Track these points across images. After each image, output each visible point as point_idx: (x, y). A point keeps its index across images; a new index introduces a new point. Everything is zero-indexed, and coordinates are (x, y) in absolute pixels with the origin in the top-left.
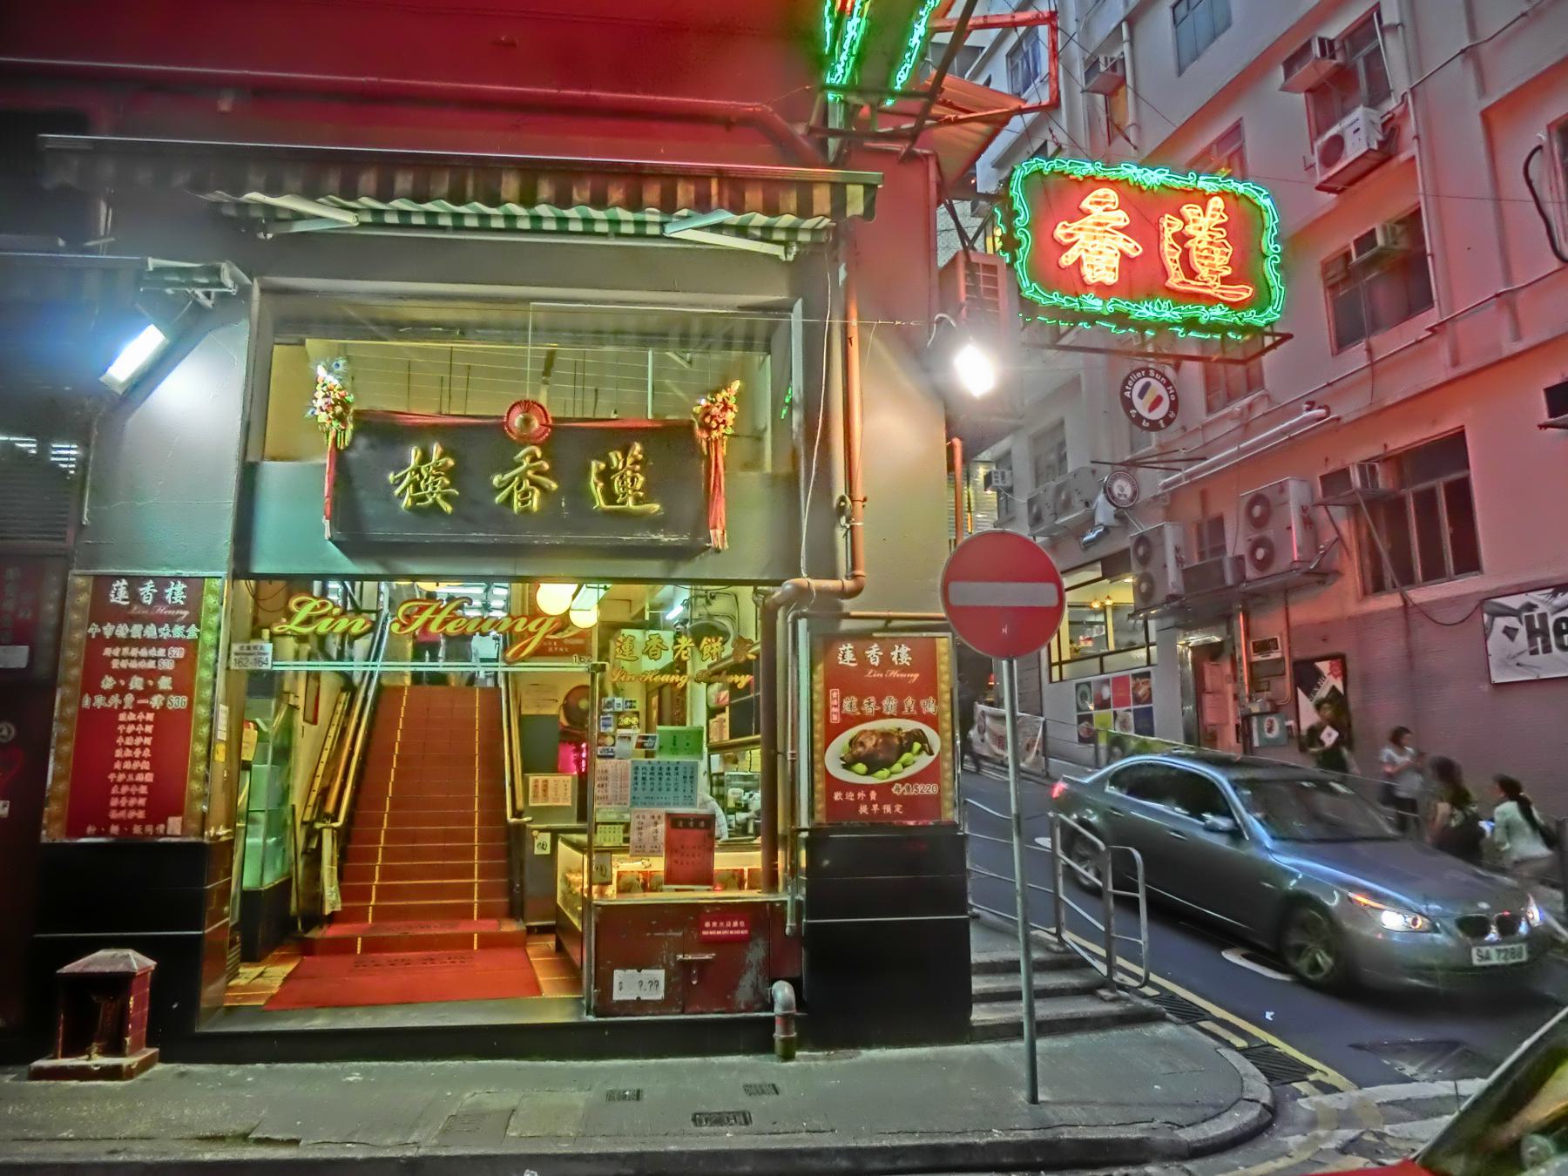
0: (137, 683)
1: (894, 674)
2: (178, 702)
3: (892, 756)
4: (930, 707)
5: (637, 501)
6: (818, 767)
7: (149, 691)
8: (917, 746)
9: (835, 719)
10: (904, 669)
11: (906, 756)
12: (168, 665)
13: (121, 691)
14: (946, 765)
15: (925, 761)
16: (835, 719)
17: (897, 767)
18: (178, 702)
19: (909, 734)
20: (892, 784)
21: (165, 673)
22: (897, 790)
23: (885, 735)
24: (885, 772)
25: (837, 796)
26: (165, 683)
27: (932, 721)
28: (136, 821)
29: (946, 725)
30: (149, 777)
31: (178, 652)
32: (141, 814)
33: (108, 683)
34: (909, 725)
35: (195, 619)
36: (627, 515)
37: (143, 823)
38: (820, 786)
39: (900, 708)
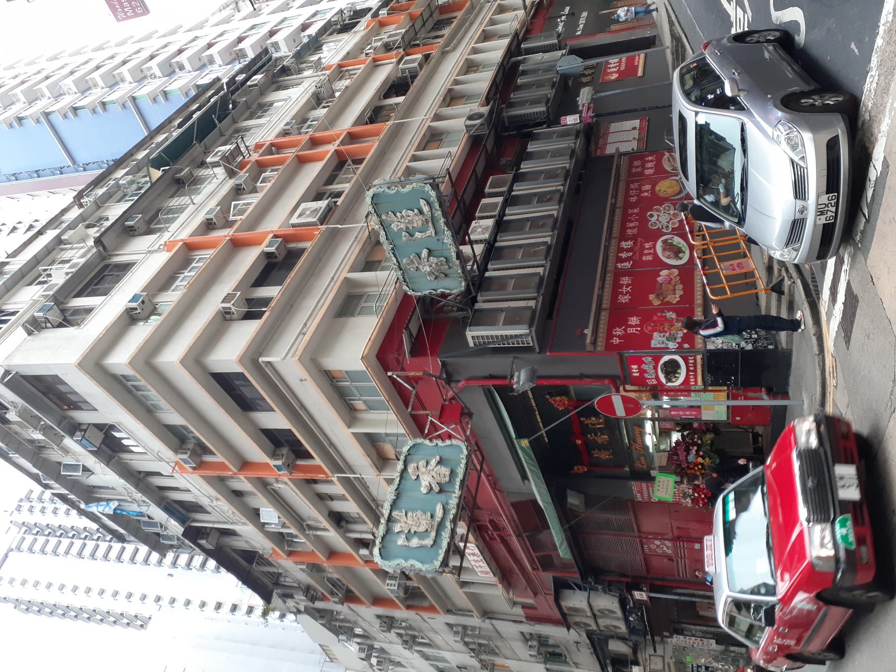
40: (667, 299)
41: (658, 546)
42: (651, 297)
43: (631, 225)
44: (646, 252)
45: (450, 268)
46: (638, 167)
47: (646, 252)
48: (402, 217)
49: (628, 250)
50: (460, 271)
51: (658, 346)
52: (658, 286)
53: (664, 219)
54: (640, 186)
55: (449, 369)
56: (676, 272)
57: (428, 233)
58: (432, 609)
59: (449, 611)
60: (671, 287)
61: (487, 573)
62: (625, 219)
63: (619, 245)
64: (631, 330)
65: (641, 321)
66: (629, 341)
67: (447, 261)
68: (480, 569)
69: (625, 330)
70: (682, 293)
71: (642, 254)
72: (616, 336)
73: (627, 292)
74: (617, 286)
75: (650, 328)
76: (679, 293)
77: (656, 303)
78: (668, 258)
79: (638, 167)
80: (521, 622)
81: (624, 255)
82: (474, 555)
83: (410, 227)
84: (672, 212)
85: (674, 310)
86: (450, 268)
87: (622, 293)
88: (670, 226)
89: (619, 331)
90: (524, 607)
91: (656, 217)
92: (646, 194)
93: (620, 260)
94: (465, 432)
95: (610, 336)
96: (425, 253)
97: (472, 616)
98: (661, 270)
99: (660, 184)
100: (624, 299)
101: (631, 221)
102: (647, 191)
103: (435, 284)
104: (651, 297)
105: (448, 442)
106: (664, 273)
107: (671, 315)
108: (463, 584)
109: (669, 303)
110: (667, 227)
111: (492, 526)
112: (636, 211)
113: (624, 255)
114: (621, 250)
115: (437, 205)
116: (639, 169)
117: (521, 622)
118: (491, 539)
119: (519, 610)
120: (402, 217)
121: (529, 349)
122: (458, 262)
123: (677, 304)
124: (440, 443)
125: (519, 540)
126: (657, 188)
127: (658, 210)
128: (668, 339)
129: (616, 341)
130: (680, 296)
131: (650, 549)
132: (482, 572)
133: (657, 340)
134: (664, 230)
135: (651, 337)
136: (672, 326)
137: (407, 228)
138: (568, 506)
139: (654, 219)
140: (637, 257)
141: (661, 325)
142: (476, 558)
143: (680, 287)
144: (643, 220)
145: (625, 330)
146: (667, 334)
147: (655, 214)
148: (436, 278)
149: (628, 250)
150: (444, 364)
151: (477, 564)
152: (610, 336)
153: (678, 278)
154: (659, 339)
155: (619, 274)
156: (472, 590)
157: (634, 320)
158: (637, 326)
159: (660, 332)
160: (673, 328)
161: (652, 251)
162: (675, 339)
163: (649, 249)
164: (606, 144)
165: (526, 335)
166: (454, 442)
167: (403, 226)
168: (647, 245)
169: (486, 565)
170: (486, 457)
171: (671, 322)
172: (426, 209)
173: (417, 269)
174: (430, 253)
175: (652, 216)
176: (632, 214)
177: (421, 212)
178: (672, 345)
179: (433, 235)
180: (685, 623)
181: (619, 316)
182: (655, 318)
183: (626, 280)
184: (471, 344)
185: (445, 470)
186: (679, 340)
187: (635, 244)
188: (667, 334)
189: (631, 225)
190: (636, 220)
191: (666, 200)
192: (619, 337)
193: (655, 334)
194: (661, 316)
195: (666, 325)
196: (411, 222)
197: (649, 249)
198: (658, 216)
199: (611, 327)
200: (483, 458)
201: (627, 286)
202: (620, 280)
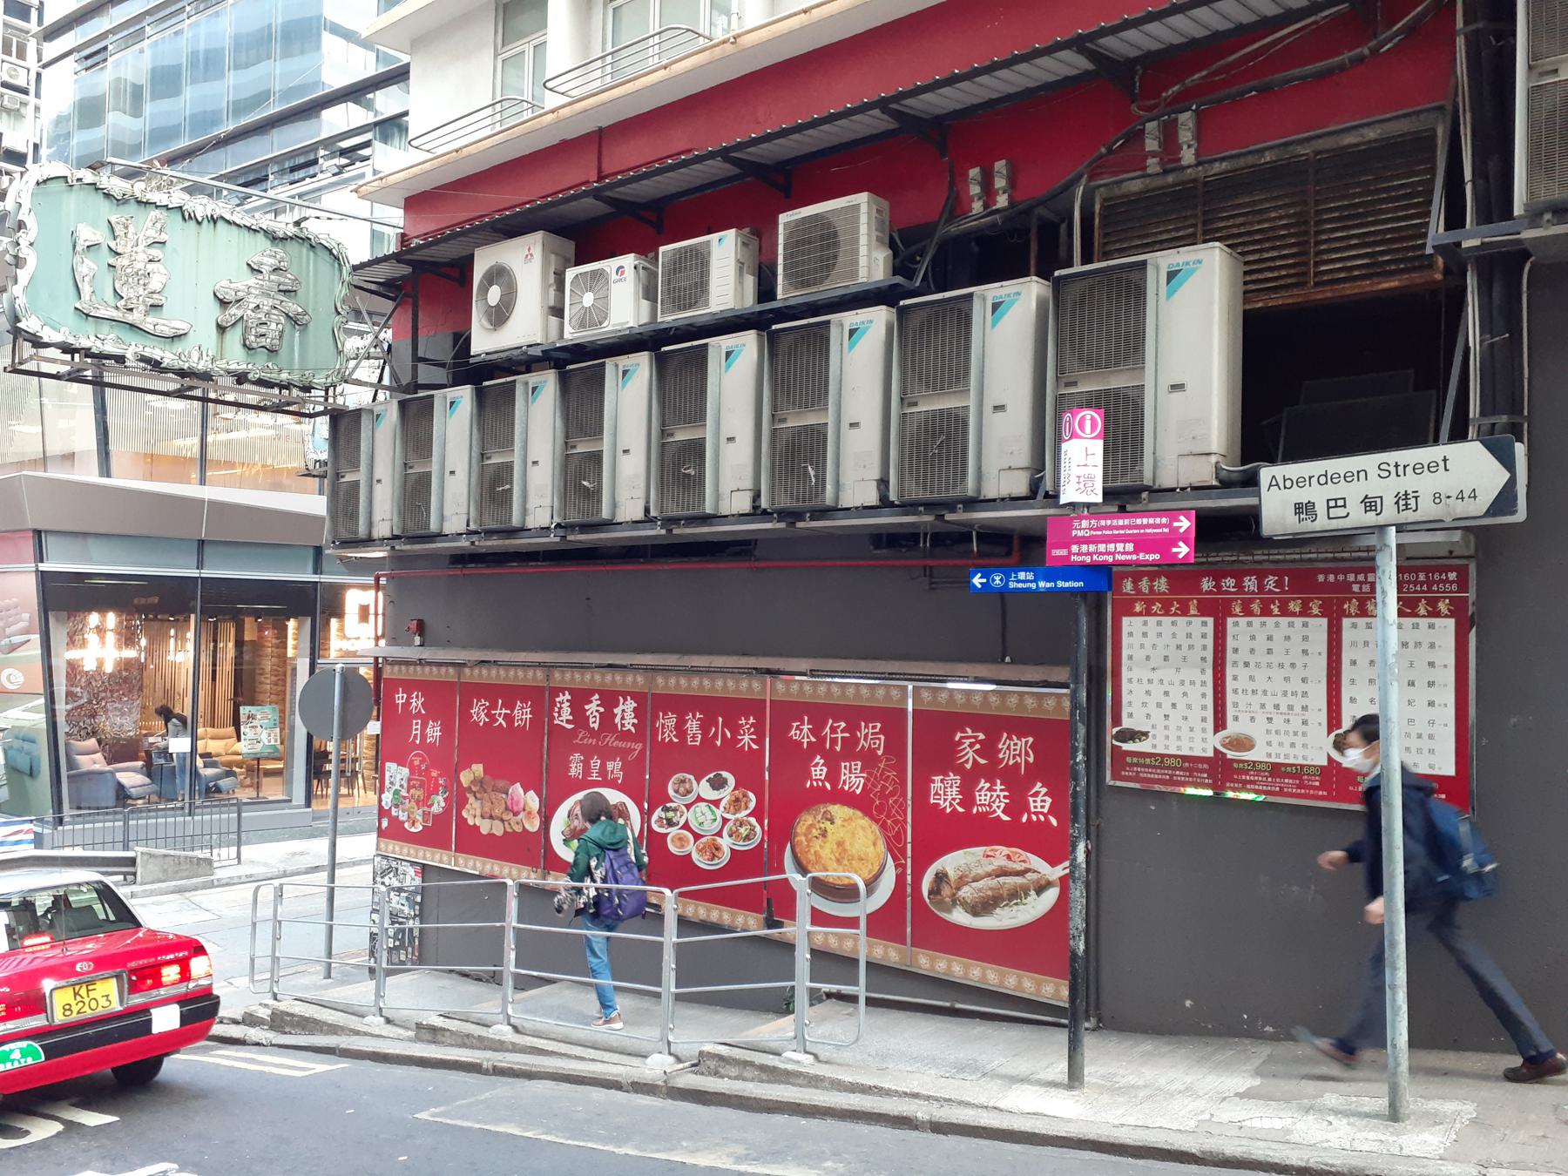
40: (471, 799)
42: (478, 769)
43: (693, 726)
44: (596, 763)
46: (989, 749)
47: (596, 763)
49: (607, 718)
51: (387, 775)
52: (501, 784)
53: (702, 818)
54: (869, 760)
56: (534, 826)
60: (497, 812)
62: (711, 708)
63: (625, 695)
64: (416, 726)
65: (432, 745)
66: (395, 721)
69: (418, 715)
70: (484, 831)
71: (588, 753)
72: (409, 698)
73: (493, 718)
74: (509, 694)
75: (416, 763)
76: (485, 827)
77: (465, 778)
79: (989, 749)
81: (593, 708)
84: (725, 842)
85: (447, 811)
87: (494, 706)
88: (673, 831)
89: (417, 703)
92: (819, 770)
93: (580, 698)
95: (409, 686)
98: (539, 794)
99: (866, 822)
100: (479, 713)
101: (704, 727)
102: (833, 776)
104: (478, 769)
106: (533, 801)
107: (438, 804)
109: (462, 802)
110: (670, 823)
112: (746, 739)
113: (593, 708)
114: (610, 699)
116: (969, 756)
123: (462, 821)
126: (839, 811)
127: (736, 803)
128: (396, 792)
129: (400, 698)
130: (476, 828)
133: (396, 774)
134: (658, 813)
135: (401, 763)
136: (417, 802)
139: (704, 789)
140: (583, 739)
141: (423, 785)
143: (498, 830)
144: (703, 761)
145: (418, 715)
146: (404, 793)
147: (726, 794)
149: (607, 718)
152: (409, 686)
153: (518, 829)
154: (399, 777)
155: (541, 698)
157: (434, 732)
158: (424, 736)
159: (409, 780)
160: (413, 804)
161: (594, 777)
162: (397, 806)
163: (603, 771)
164: (1218, 611)
168: (614, 766)
171: (425, 802)
175: (718, 784)
176: (736, 730)
178: (387, 797)
181: (445, 698)
182: (434, 774)
183: (523, 714)
186: (394, 812)
187: (626, 735)
188: (404, 793)
189: (693, 726)
190: (707, 741)
191: (781, 832)
192: (407, 704)
193: (406, 771)
194: (437, 786)
195: (418, 793)
197: (603, 771)
198: (716, 803)
199: (425, 687)
201: (509, 718)
202: (524, 701)
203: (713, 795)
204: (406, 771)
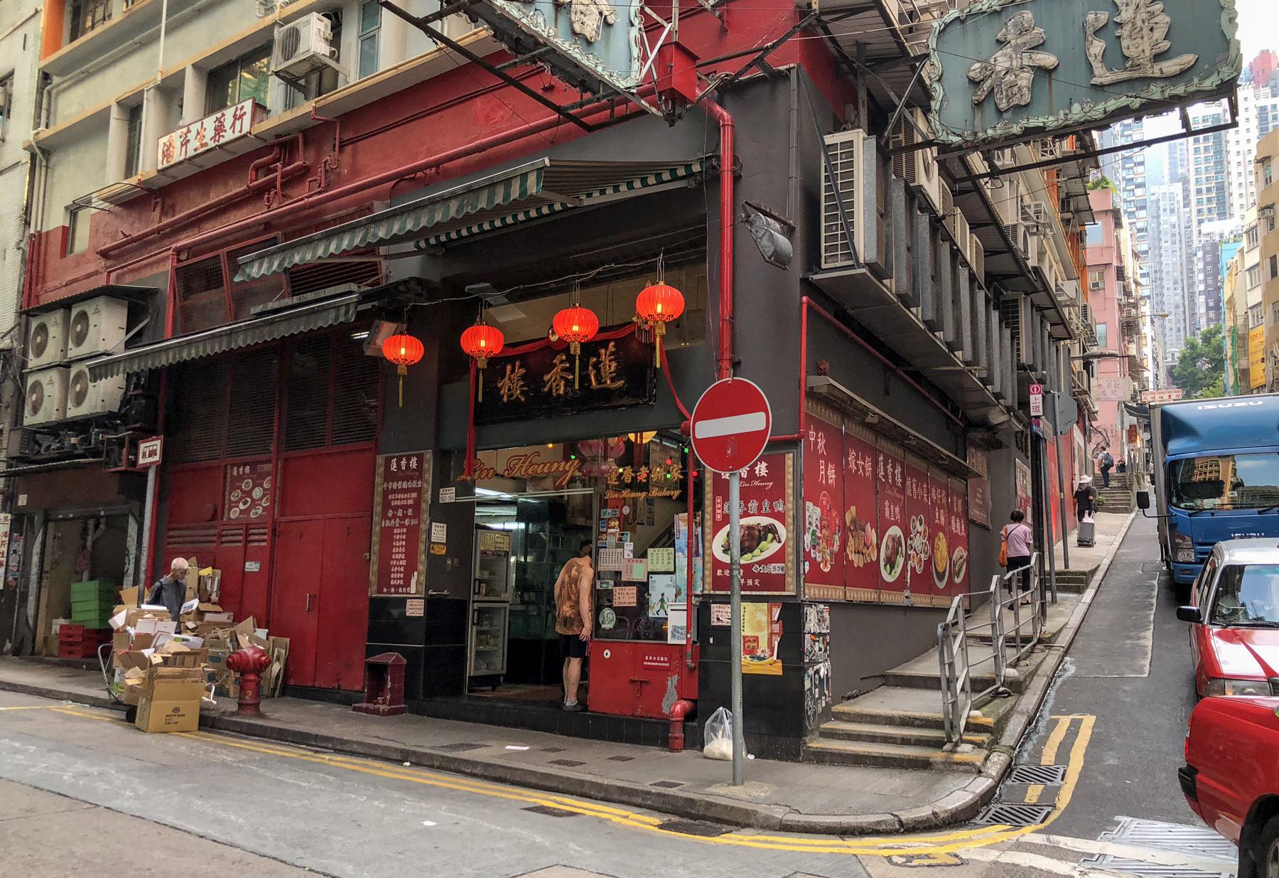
0: (400, 514)
1: (756, 483)
2: (414, 522)
3: (755, 543)
4: (779, 507)
5: (613, 380)
6: (708, 552)
7: (405, 516)
8: (770, 536)
9: (719, 517)
10: (762, 479)
11: (763, 544)
12: (411, 502)
13: (395, 517)
14: (789, 550)
15: (775, 547)
16: (719, 517)
17: (757, 551)
18: (414, 522)
19: (765, 527)
20: (752, 565)
21: (410, 506)
22: (756, 569)
23: (750, 528)
24: (749, 555)
25: (719, 572)
26: (410, 512)
27: (781, 517)
28: (400, 586)
29: (790, 520)
30: (404, 563)
31: (414, 495)
32: (401, 582)
33: (390, 514)
34: (765, 521)
35: (420, 477)
36: (607, 389)
37: (402, 586)
38: (709, 566)
39: (760, 508)
41: (249, 494)
42: (853, 509)
45: (1000, 112)
48: (1152, 15)
50: (990, 132)
55: (761, 91)
57: (1099, 68)
58: (52, 42)
59: (45, 77)
61: (167, 155)
67: (1018, 107)
68: (177, 143)
78: (887, 546)
80: (27, 223)
82: (219, 129)
83: (1125, 32)
86: (1000, 112)
90: (67, 234)
91: (920, 528)
94: (643, 94)
96: (1047, 59)
97: (37, 125)
103: (957, 80)
105: (636, 52)
108: (132, 110)
111: (295, 170)
115: (1180, 90)
117: (27, 223)
118: (257, 169)
119: (56, 219)
120: (1152, 15)
121: (812, 260)
122: (1016, 129)
124: (634, 32)
125: (258, 223)
131: (241, 478)
132: (169, 146)
135: (816, 504)
137: (1120, 25)
138: (377, 321)
142: (210, 132)
148: (975, 83)
150: (784, 76)
151: (191, 136)
152: (820, 426)
156: (116, 127)
157: (832, 474)
165: (852, 255)
166: (636, 65)
167: (1126, 15)
169: (191, 153)
170: (591, 134)
171: (830, 543)
172: (1170, 67)
173: (1001, 43)
174: (1043, 72)
177: (1159, 57)
179: (1096, 81)
180: (45, 534)
184: (829, 139)
185: (590, 26)
188: (818, 534)
192: (816, 443)
196: (1136, 32)
200: (590, 129)
203: (920, 528)
204: (819, 510)
